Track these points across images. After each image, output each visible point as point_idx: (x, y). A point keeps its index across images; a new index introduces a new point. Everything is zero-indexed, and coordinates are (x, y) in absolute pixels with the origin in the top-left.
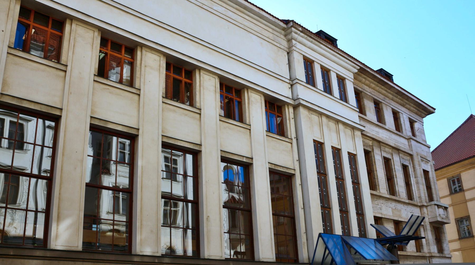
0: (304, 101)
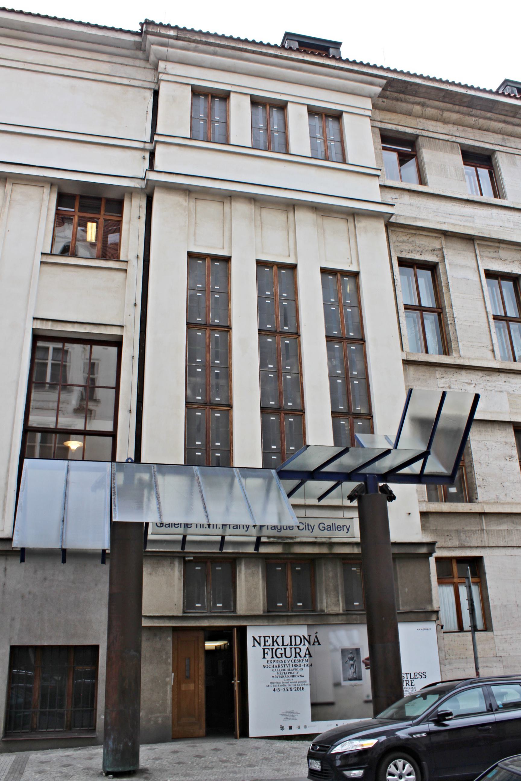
0: (163, 174)
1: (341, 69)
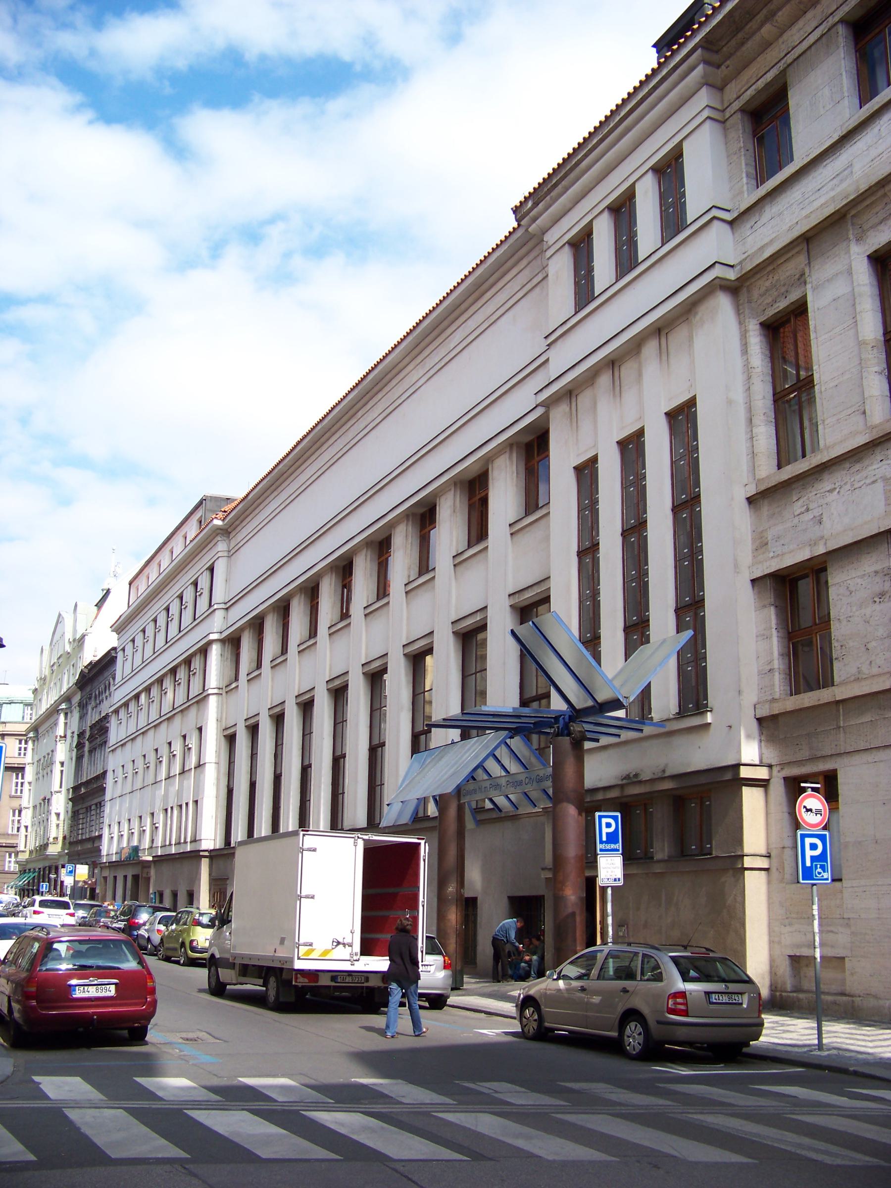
1: (655, 88)
